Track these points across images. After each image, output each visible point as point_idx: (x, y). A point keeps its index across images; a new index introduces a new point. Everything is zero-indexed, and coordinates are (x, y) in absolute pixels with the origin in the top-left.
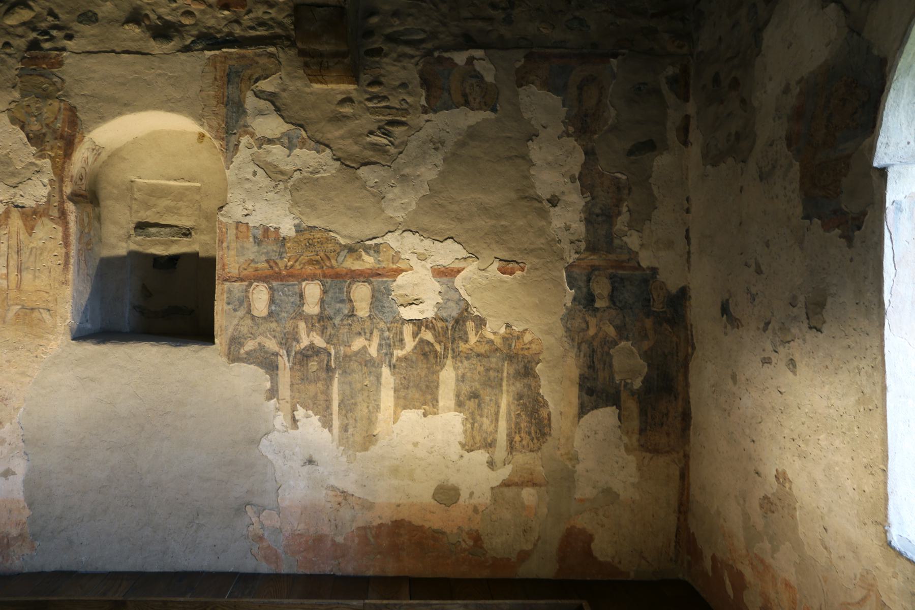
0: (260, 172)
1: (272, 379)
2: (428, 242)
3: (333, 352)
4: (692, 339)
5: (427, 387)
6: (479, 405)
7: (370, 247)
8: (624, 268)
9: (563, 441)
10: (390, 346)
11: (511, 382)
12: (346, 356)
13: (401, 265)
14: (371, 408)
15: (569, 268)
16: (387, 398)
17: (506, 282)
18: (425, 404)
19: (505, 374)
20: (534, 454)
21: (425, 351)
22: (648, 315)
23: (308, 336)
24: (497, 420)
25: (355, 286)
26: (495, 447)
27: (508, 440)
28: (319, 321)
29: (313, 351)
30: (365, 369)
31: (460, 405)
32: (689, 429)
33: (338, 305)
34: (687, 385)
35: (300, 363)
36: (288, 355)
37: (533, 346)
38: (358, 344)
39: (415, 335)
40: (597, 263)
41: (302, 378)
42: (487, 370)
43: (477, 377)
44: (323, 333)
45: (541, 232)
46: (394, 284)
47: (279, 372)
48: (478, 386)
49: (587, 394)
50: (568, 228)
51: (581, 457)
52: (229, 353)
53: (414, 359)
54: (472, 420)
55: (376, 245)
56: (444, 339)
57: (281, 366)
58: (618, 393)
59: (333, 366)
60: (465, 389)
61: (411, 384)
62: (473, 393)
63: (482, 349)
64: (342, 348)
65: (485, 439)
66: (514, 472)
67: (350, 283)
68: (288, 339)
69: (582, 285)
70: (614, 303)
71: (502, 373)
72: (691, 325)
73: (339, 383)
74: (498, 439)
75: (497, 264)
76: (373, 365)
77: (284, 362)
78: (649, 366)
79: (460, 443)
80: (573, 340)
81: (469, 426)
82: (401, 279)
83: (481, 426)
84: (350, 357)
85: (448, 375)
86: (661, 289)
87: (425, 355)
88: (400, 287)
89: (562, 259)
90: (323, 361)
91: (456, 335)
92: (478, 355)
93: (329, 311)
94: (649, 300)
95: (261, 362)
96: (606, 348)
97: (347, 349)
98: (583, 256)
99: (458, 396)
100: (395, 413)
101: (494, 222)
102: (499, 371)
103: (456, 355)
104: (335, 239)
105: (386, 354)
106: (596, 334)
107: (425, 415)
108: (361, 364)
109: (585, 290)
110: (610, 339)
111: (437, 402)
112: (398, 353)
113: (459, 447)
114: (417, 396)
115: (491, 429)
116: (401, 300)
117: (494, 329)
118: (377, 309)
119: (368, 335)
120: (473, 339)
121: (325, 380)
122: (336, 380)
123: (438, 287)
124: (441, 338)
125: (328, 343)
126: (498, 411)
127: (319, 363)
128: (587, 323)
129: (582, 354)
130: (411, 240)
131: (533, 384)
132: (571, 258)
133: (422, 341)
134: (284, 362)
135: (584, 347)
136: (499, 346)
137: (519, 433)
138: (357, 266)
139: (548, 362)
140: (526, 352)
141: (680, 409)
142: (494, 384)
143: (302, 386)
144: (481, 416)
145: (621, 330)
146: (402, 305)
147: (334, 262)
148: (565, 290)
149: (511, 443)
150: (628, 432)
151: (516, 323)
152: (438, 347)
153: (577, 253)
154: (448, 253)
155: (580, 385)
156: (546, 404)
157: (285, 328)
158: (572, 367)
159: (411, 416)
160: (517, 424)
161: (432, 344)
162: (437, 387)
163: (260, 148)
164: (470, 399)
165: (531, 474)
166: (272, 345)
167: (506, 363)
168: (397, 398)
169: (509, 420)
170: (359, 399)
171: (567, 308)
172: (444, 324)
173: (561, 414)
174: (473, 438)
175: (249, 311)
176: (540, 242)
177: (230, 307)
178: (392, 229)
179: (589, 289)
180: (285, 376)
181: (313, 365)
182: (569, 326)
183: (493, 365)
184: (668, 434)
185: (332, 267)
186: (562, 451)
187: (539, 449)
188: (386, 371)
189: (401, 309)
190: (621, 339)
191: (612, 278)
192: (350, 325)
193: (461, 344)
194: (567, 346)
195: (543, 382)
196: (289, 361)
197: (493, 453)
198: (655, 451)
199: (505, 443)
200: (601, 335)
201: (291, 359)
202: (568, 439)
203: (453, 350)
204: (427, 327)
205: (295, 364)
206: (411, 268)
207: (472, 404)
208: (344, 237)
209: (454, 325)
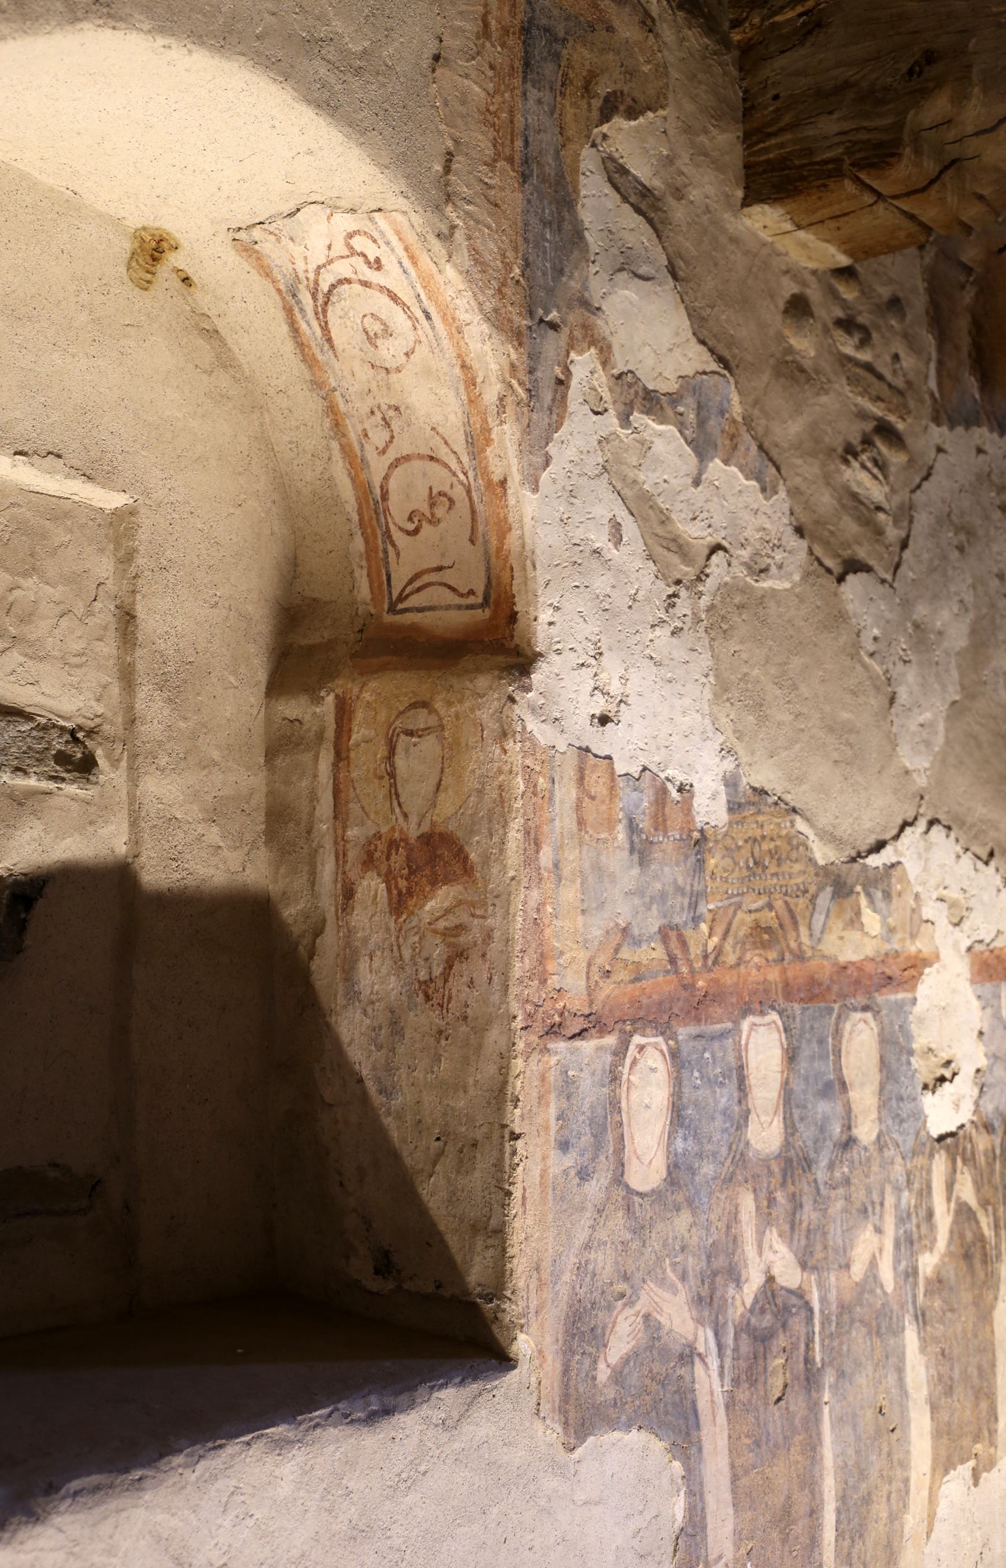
0: (630, 528)
163: (625, 420)
175: (619, 1178)
177: (569, 1160)
196: (721, 1375)
205: (736, 1381)
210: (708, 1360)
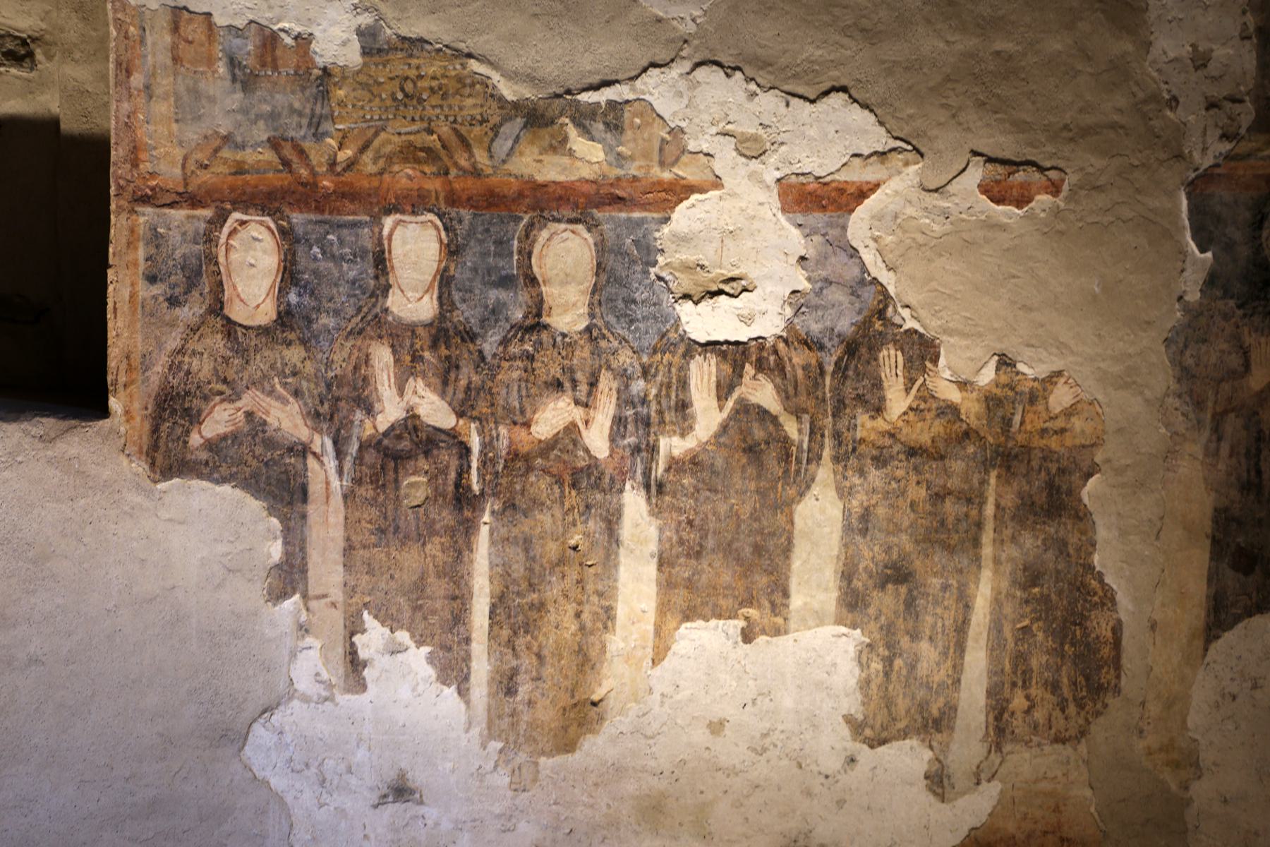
1: (287, 531)
2: (769, 102)
3: (475, 443)
5: (758, 549)
6: (910, 604)
7: (593, 111)
9: (1154, 709)
10: (648, 424)
11: (1008, 532)
12: (514, 455)
13: (687, 172)
14: (586, 616)
15: (1198, 187)
16: (636, 585)
17: (1003, 228)
18: (749, 601)
19: (990, 509)
20: (1066, 750)
21: (751, 438)
23: (401, 392)
24: (961, 648)
25: (545, 234)
26: (952, 729)
27: (990, 708)
28: (434, 346)
29: (413, 440)
30: (572, 498)
31: (853, 604)
33: (494, 295)
35: (374, 480)
36: (340, 454)
37: (1077, 423)
38: (552, 416)
39: (724, 390)
41: (380, 526)
42: (938, 497)
43: (906, 519)
44: (445, 383)
45: (1118, 74)
46: (666, 230)
47: (311, 509)
48: (909, 547)
49: (1235, 567)
50: (1200, 61)
51: (1207, 757)
52: (155, 447)
53: (719, 463)
54: (886, 649)
55: (612, 104)
56: (810, 404)
57: (315, 488)
59: (476, 488)
60: (871, 554)
61: (710, 543)
62: (895, 566)
63: (924, 433)
64: (503, 430)
65: (923, 707)
66: (1005, 804)
67: (531, 225)
68: (340, 401)
69: (1237, 236)
71: (982, 504)
73: (493, 543)
74: (962, 706)
75: (976, 173)
76: (597, 485)
77: (326, 476)
79: (849, 719)
80: (1199, 405)
81: (877, 666)
82: (685, 216)
83: (912, 667)
84: (527, 458)
85: (820, 515)
87: (752, 450)
88: (682, 240)
89: (1179, 156)
90: (444, 471)
91: (849, 390)
92: (912, 452)
93: (466, 314)
95: (255, 475)
97: (521, 434)
98: (1244, 147)
99: (847, 576)
100: (658, 631)
101: (971, 43)
102: (973, 498)
103: (848, 453)
104: (485, 82)
105: (636, 450)
107: (747, 636)
108: (560, 481)
109: (1244, 252)
111: (786, 594)
112: (672, 445)
113: (845, 731)
114: (726, 578)
115: (940, 676)
116: (684, 283)
117: (964, 372)
118: (613, 310)
119: (583, 388)
120: (897, 401)
121: (451, 532)
122: (484, 530)
123: (796, 241)
124: (803, 399)
125: (460, 415)
126: (966, 622)
127: (432, 479)
128: (1246, 353)
129: (1225, 449)
130: (720, 93)
131: (1073, 539)
132: (1207, 152)
133: (745, 409)
134: (326, 476)
135: (1232, 425)
136: (974, 423)
137: (1025, 686)
138: (552, 171)
139: (1119, 471)
140: (1053, 443)
142: (952, 535)
143: (379, 554)
144: (915, 636)
146: (686, 296)
147: (481, 156)
148: (1183, 253)
149: (998, 718)
151: (1028, 353)
152: (791, 428)
153: (1225, 137)
154: (829, 138)
155: (1215, 541)
156: (1108, 599)
157: (329, 364)
158: (1193, 487)
159: (705, 639)
160: (1020, 659)
161: (774, 419)
162: (787, 550)
164: (883, 586)
165: (1057, 809)
166: (287, 419)
167: (994, 474)
168: (667, 585)
169: (995, 648)
170: (553, 590)
171: (1187, 309)
172: (811, 357)
173: (1153, 626)
174: (889, 703)
176: (1114, 105)
178: (662, 56)
180: (327, 522)
181: (415, 485)
182: (1190, 362)
183: (954, 483)
185: (476, 173)
186: (1152, 740)
187: (1083, 733)
188: (634, 502)
189: (686, 310)
192: (531, 358)
193: (863, 418)
194: (1180, 424)
195: (1103, 533)
196: (340, 471)
197: (945, 747)
199: (982, 718)
201: (348, 465)
202: (1169, 705)
203: (837, 436)
204: (760, 366)
205: (358, 481)
206: (717, 183)
207: (887, 601)
208: (511, 76)
209: (844, 355)
210: (325, 459)
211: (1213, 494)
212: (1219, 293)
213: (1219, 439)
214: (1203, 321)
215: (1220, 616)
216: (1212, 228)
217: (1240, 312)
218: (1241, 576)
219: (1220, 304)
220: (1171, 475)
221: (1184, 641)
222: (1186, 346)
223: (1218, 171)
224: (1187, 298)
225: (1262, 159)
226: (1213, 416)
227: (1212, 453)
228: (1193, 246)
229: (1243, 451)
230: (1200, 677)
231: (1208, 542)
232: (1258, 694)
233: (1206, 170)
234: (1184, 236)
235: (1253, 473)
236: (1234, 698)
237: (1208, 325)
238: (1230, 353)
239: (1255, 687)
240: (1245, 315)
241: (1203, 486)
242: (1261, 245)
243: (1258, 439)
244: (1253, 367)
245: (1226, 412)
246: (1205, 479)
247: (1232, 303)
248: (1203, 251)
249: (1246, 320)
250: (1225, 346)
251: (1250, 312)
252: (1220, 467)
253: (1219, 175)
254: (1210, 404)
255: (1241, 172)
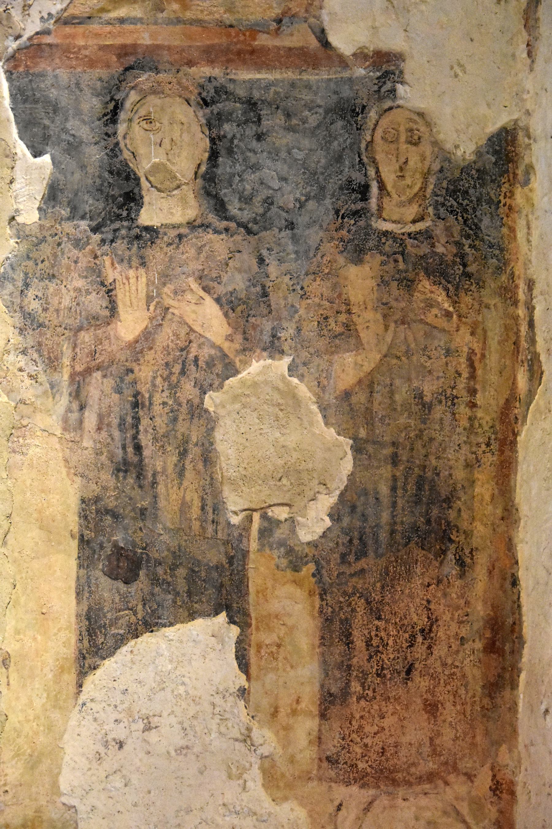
4: (533, 341)
8: (254, 56)
22: (358, 254)
32: (514, 685)
34: (509, 514)
40: (145, 39)
49: (112, 575)
58: (235, 562)
69: (84, 132)
70: (220, 207)
72: (531, 284)
78: (358, 449)
80: (52, 363)
86: (415, 143)
94: (363, 191)
96: (188, 390)
106: (147, 336)
109: (95, 155)
110: (206, 353)
129: (91, 419)
135: (99, 388)
141: (480, 610)
145: (247, 310)
148: (13, 157)
150: (275, 713)
155: (83, 542)
171: (21, 233)
179: (114, 151)
182: (34, 306)
184: (432, 708)
190: (247, 350)
191: (209, 99)
194: (28, 390)
198: (385, 775)
200: (165, 337)
202: (33, 763)
211: (78, 480)
212: (65, 212)
213: (82, 408)
214: (46, 250)
215: (96, 641)
216: (47, 122)
217: (97, 237)
218: (120, 585)
219: (68, 227)
220: (18, 457)
221: (50, 676)
222: (27, 285)
223: (48, 40)
224: (20, 219)
225: (109, 23)
226: (72, 376)
227: (73, 426)
228: (21, 148)
229: (115, 422)
230: (73, 722)
231: (74, 544)
232: (153, 736)
233: (30, 39)
234: (11, 134)
235: (130, 450)
236: (121, 745)
237: (55, 255)
238: (88, 292)
239: (148, 728)
240: (103, 241)
241: (64, 471)
242: (117, 144)
243: (136, 405)
244: (121, 308)
245: (88, 371)
246: (66, 461)
247: (84, 225)
248: (36, 154)
249: (106, 247)
250: (80, 283)
251: (110, 236)
252: (85, 444)
253: (50, 45)
254: (66, 361)
255: (81, 42)
